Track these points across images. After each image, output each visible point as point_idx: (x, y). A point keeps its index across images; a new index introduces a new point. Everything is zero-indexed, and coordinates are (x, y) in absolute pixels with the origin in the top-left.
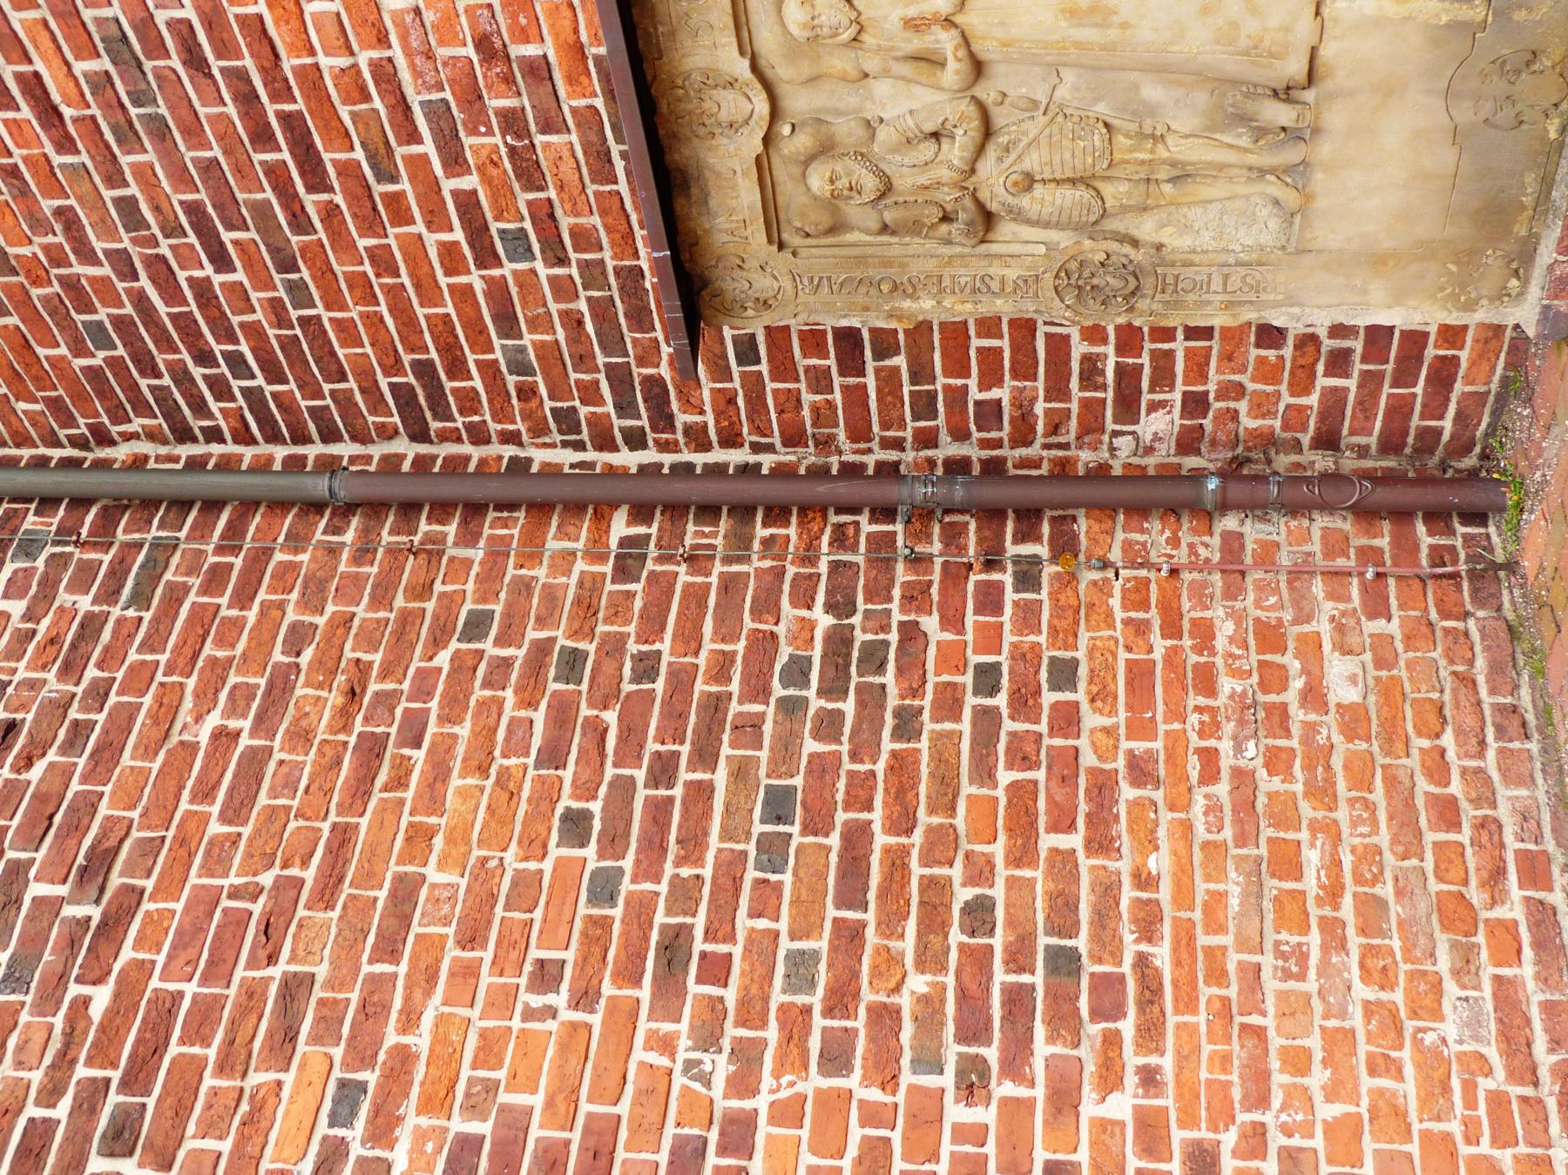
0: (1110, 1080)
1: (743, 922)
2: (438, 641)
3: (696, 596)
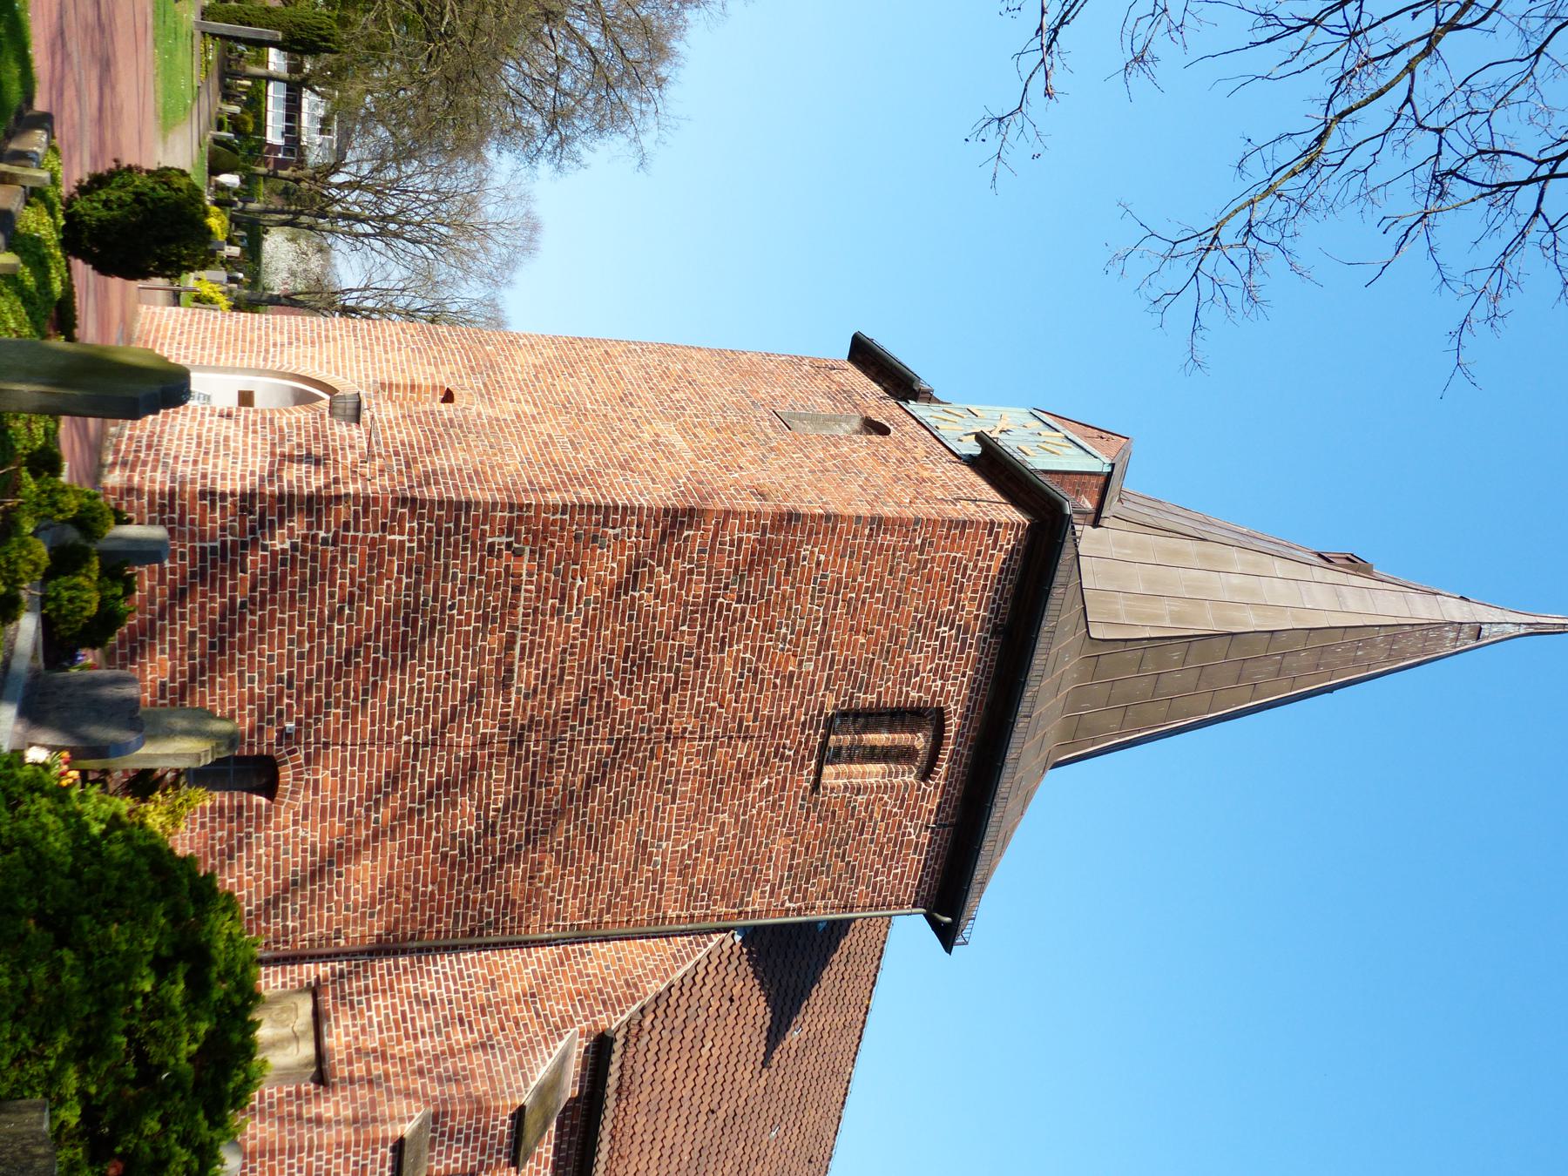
0: (221, 838)
1: (300, 859)
2: (380, 911)
3: (321, 926)
